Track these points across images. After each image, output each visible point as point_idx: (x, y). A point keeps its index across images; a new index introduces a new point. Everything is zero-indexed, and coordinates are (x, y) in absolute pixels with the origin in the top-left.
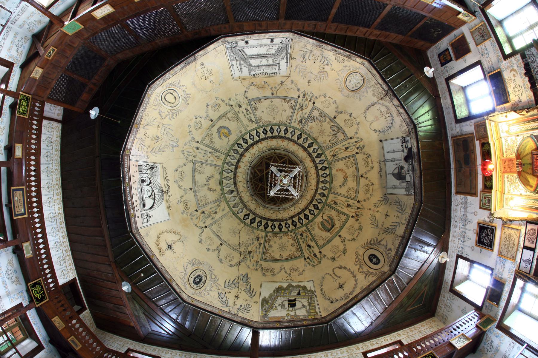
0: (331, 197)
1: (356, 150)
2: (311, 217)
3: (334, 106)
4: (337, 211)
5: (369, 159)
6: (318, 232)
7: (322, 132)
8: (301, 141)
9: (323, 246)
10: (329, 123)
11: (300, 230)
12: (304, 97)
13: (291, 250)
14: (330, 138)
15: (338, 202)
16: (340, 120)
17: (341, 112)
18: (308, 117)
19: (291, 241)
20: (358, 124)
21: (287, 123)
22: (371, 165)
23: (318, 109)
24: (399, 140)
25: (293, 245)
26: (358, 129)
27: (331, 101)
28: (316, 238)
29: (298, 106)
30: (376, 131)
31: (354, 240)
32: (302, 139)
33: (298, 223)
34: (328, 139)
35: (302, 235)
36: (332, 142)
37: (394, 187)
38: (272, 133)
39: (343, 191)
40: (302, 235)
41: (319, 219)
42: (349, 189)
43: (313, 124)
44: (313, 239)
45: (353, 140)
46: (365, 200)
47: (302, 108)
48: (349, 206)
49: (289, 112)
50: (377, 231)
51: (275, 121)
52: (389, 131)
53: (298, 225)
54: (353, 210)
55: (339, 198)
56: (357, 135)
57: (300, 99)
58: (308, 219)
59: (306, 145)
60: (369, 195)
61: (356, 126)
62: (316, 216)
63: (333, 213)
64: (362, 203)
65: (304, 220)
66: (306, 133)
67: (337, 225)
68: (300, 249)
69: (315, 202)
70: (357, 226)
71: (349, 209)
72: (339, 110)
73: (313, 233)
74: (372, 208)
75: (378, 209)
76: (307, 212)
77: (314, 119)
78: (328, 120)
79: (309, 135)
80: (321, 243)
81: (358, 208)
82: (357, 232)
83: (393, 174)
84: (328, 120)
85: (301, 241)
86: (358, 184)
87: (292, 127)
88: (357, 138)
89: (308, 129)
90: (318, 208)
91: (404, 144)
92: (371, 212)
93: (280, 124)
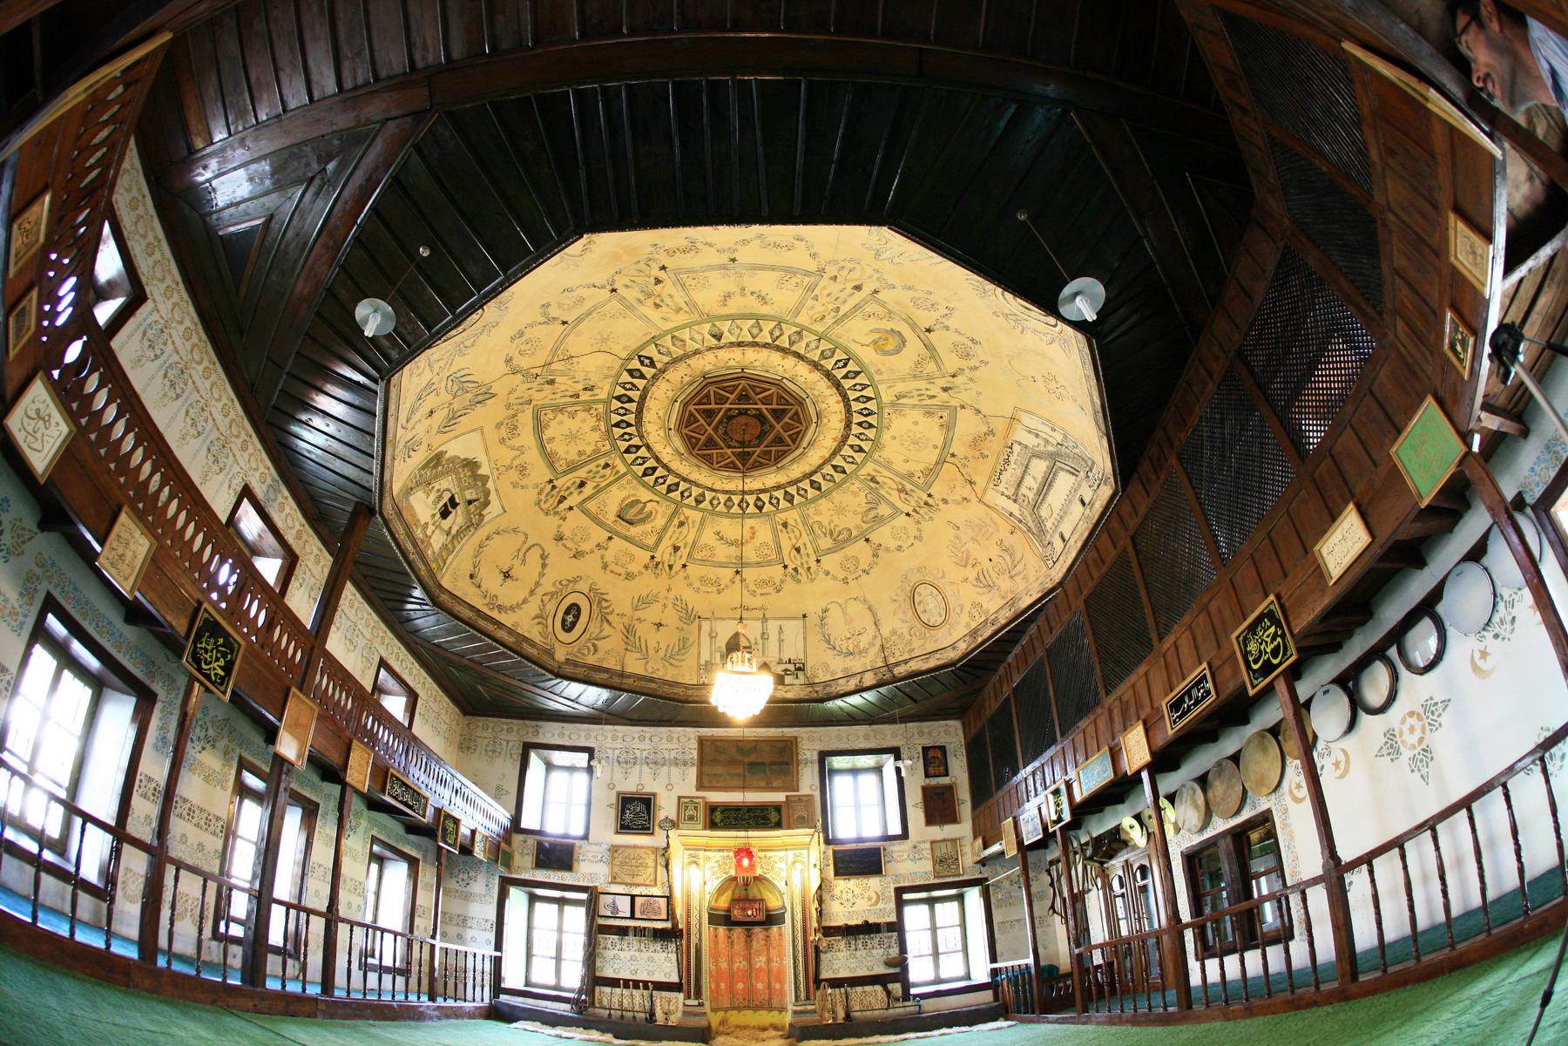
0: (695, 515)
1: (791, 566)
2: (650, 480)
3: (893, 544)
4: (665, 529)
5: (770, 590)
6: (614, 499)
7: (841, 510)
8: (828, 469)
9: (585, 512)
10: (858, 527)
11: (618, 462)
12: (926, 504)
13: (566, 452)
14: (825, 524)
15: (684, 529)
16: (860, 549)
17: (875, 555)
18: (879, 494)
19: (589, 450)
20: (845, 580)
21: (876, 456)
22: (759, 591)
23: (892, 517)
24: (801, 656)
25: (580, 453)
26: (835, 578)
27: (905, 546)
28: (602, 496)
29: (908, 487)
30: (825, 611)
31: (605, 566)
32: (832, 472)
33: (633, 456)
34: (824, 519)
35: (606, 466)
36: (816, 527)
37: (713, 636)
38: (860, 424)
39: (708, 537)
40: (606, 466)
41: (644, 495)
42: (711, 548)
43: (862, 499)
44: (599, 490)
45: (813, 564)
46: (687, 577)
47: (902, 490)
48: (676, 549)
49: (902, 468)
50: (627, 610)
51: (886, 437)
52: (820, 637)
53: (630, 457)
54: (666, 557)
55: (693, 532)
56: (822, 575)
57: (925, 497)
58: (645, 474)
59: (817, 478)
60: (697, 584)
61: (841, 577)
62: (652, 488)
63: (659, 522)
64: (682, 574)
65: (642, 468)
66: (844, 481)
67: (634, 531)
68: (572, 468)
69: (683, 485)
70: (634, 568)
71: (670, 550)
72: (880, 552)
73: (614, 488)
74: (672, 595)
75: (670, 606)
76: (660, 472)
77: (873, 505)
78: (865, 526)
79: (838, 486)
80: (592, 506)
81: (671, 567)
82: (622, 571)
83: (737, 635)
84: (865, 526)
85: (592, 466)
86: (721, 565)
87: (864, 462)
88: (817, 572)
89: (854, 488)
90: (669, 490)
91: (791, 667)
92: (664, 593)
93: (876, 442)
